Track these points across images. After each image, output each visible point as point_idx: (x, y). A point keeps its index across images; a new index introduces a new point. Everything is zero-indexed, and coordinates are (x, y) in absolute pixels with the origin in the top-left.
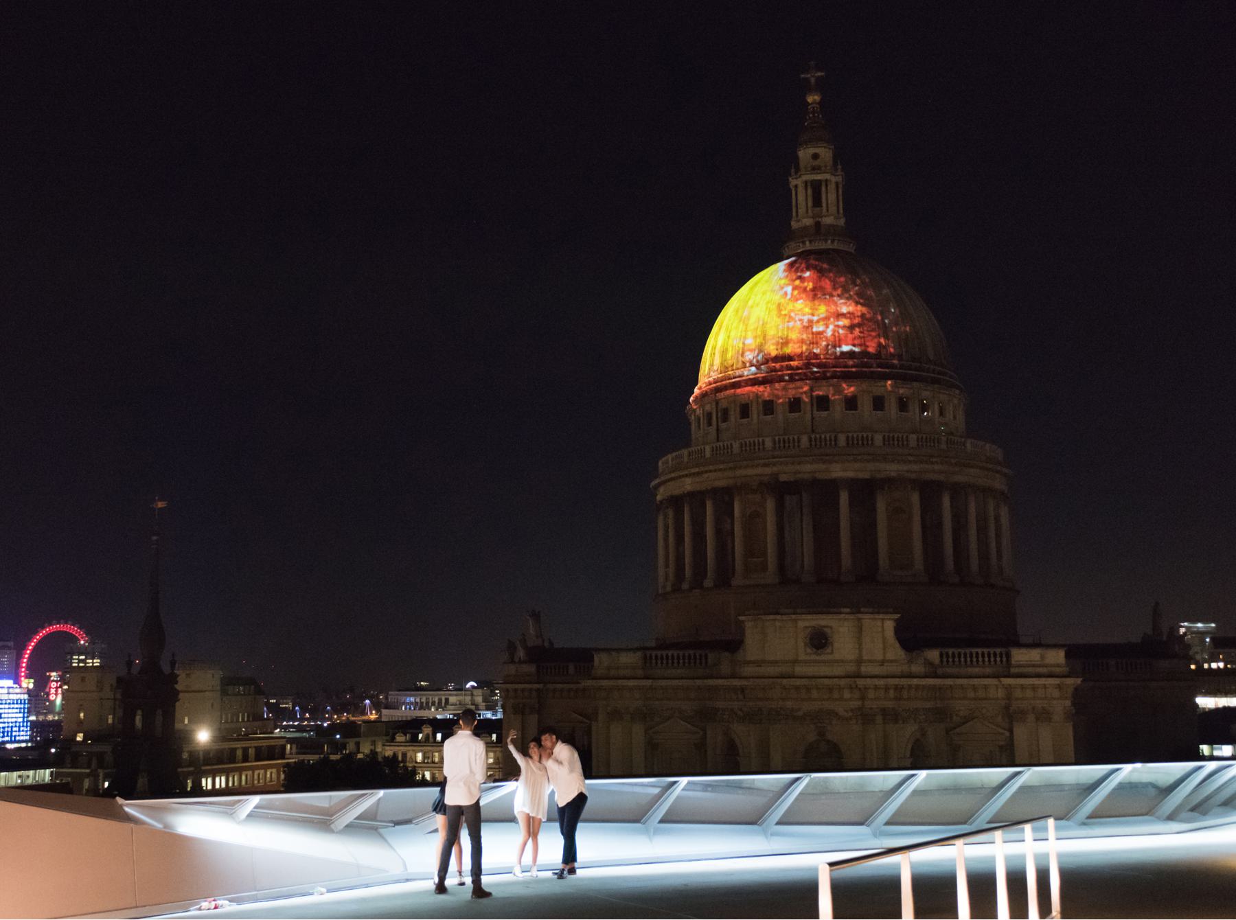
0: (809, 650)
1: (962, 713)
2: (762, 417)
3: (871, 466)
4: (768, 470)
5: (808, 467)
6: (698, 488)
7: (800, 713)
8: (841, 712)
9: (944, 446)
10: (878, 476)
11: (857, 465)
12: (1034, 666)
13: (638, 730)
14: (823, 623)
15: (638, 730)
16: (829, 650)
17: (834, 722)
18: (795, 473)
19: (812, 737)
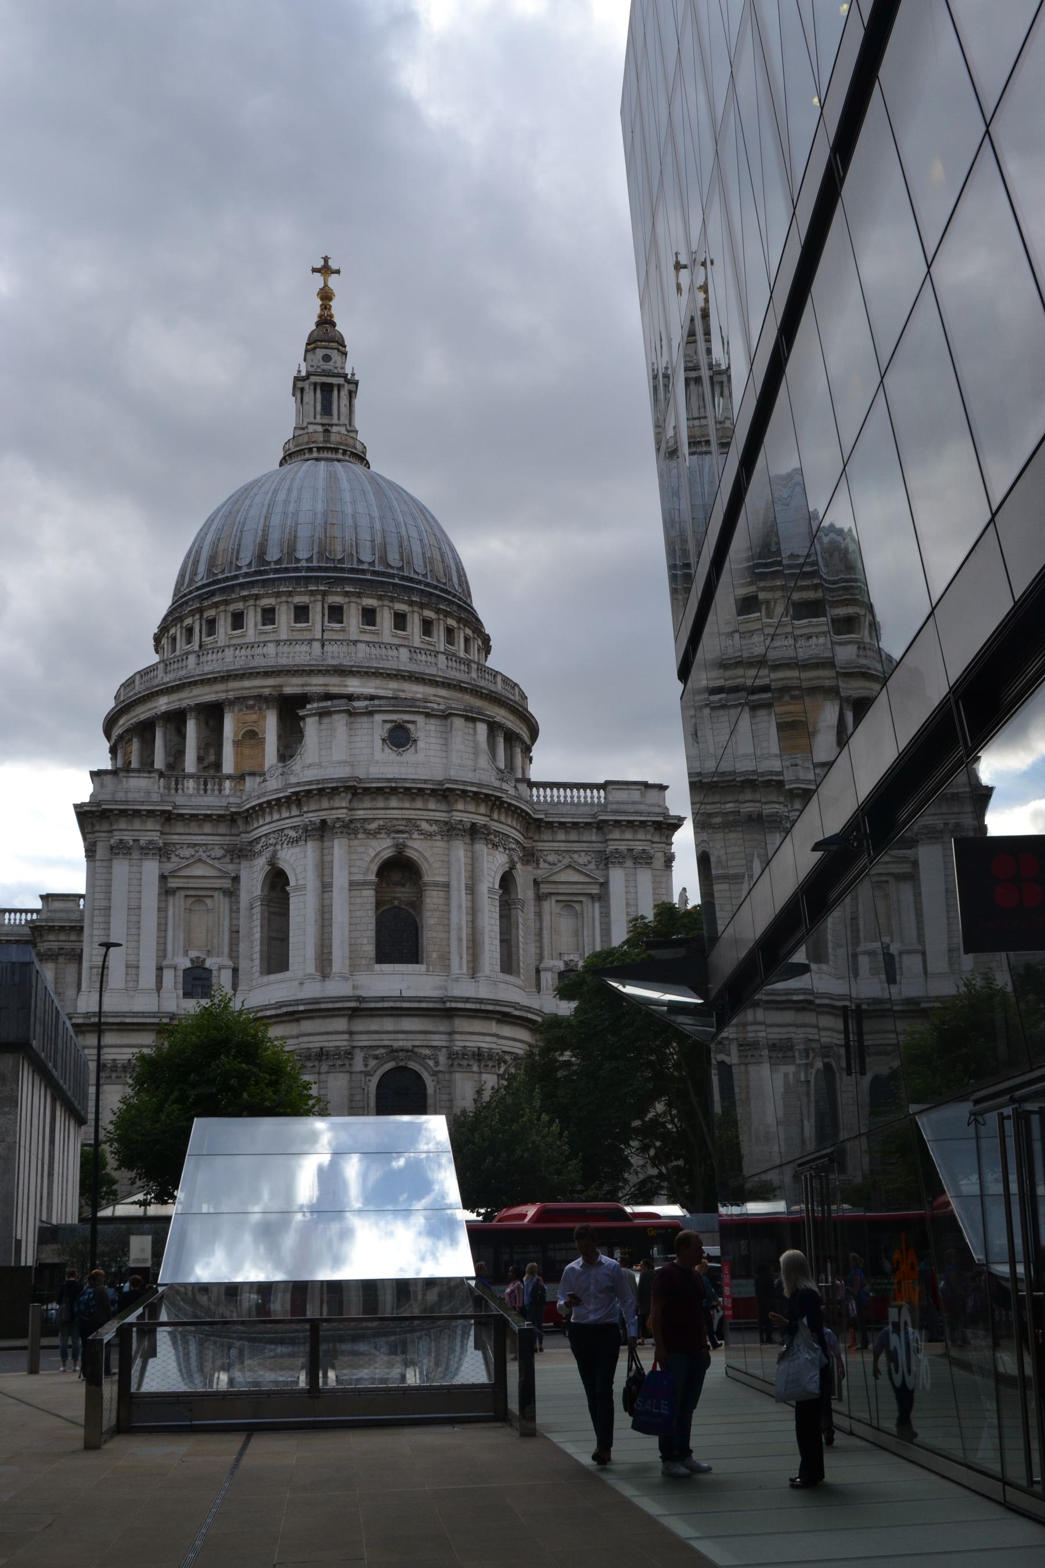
0: (387, 750)
1: (551, 858)
2: (260, 627)
3: (393, 685)
4: (270, 682)
5: (320, 680)
6: (172, 707)
7: (373, 826)
8: (424, 826)
9: (474, 675)
10: (402, 695)
11: (378, 682)
12: (634, 803)
13: (151, 869)
14: (407, 717)
15: (151, 869)
16: (412, 749)
17: (416, 836)
18: (303, 685)
19: (387, 854)
